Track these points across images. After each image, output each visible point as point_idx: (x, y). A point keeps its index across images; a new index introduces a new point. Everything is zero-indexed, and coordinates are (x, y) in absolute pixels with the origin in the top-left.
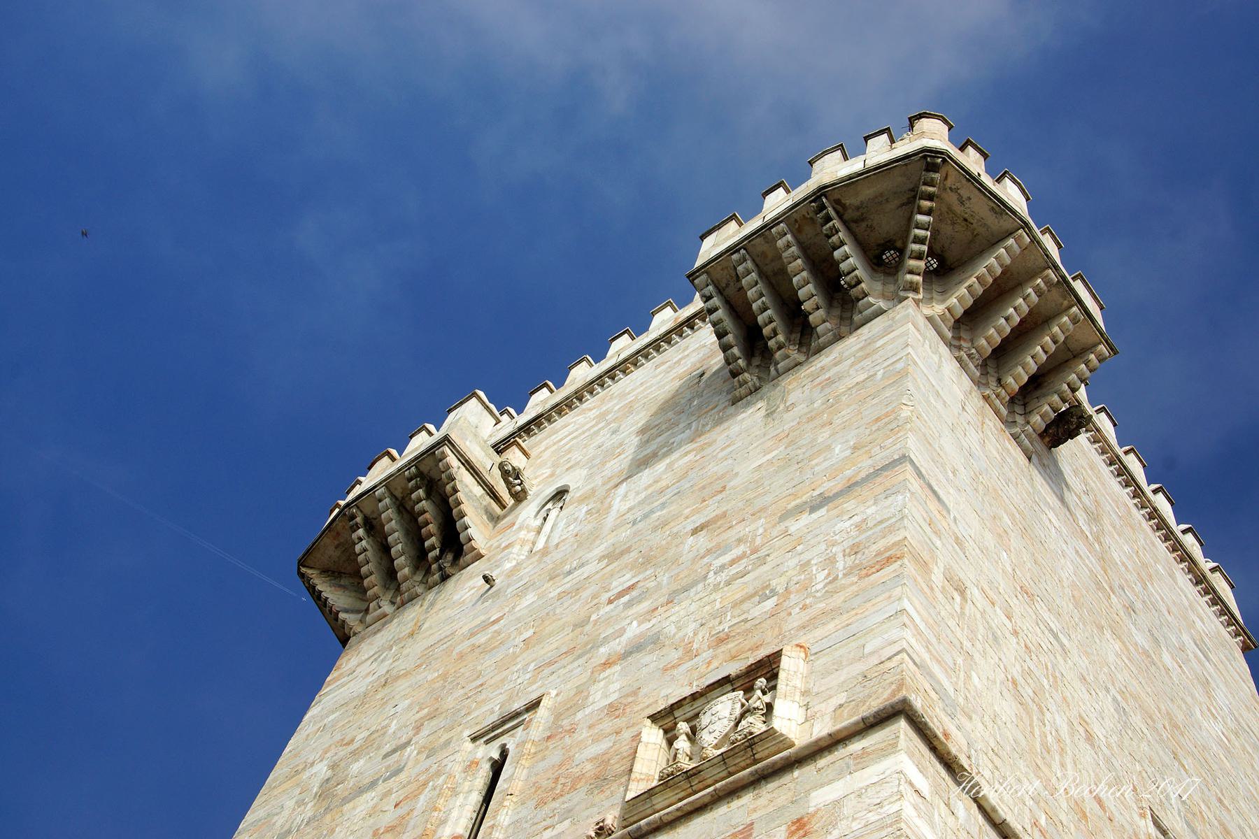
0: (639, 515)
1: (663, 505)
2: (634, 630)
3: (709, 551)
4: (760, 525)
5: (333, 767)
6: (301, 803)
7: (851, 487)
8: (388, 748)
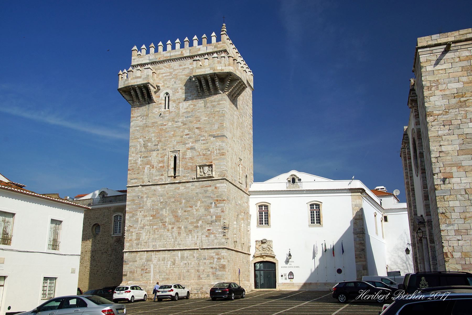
0: (186, 116)
2: (191, 144)
4: (206, 134)
5: (144, 141)
6: (141, 146)
7: (218, 136)
8: (154, 143)
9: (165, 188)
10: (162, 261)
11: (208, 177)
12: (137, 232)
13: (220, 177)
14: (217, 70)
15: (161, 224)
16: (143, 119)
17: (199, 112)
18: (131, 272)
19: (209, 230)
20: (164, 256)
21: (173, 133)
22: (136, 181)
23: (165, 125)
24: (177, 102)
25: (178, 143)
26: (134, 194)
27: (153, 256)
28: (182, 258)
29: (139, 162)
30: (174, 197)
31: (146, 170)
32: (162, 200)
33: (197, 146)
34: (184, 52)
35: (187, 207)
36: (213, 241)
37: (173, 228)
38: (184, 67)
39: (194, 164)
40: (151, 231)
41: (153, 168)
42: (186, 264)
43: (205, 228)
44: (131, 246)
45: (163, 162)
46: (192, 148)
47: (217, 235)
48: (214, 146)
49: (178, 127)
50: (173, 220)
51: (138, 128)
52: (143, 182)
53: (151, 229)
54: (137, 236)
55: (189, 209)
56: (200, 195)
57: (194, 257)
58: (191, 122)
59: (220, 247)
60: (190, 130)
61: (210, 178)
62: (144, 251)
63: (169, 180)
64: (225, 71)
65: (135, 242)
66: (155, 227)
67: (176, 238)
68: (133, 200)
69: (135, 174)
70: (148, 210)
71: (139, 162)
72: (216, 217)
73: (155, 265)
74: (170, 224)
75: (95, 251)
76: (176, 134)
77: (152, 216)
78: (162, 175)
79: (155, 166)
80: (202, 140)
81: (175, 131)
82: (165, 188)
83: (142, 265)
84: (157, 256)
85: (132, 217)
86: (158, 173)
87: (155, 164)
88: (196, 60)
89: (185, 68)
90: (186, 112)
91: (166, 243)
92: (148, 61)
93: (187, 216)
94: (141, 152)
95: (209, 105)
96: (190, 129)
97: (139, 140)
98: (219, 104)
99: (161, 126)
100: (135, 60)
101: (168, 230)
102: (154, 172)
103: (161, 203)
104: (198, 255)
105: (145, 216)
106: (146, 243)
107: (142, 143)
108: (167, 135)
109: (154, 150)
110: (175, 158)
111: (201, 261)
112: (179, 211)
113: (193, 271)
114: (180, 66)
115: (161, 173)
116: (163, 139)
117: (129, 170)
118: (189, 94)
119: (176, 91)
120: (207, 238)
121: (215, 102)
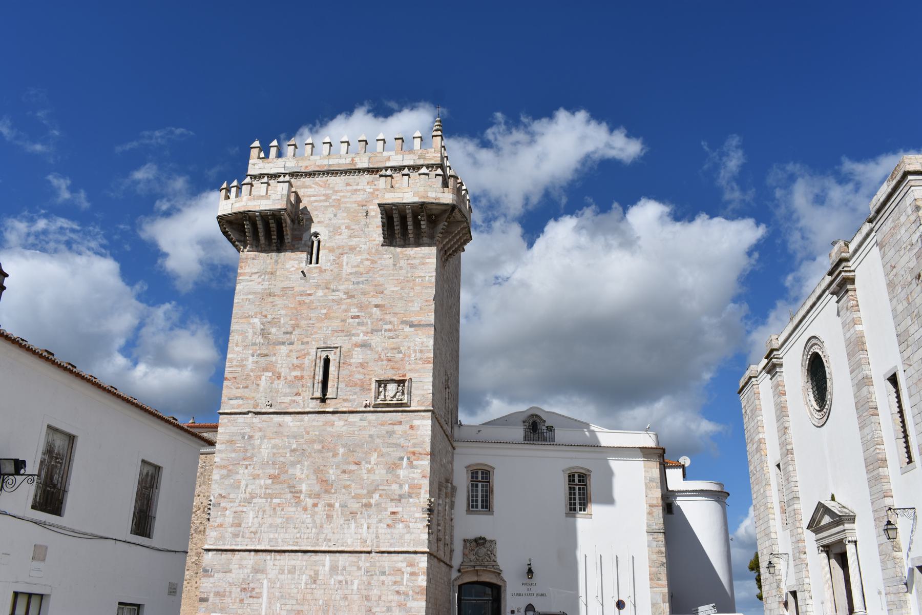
0: (355, 280)
1: (363, 283)
2: (362, 337)
3: (381, 320)
4: (395, 320)
6: (255, 333)
8: (283, 330)
9: (302, 421)
10: (289, 572)
11: (396, 405)
12: (234, 510)
13: (421, 405)
14: (427, 197)
15: (289, 496)
16: (263, 280)
17: (382, 276)
18: (217, 594)
19: (393, 513)
20: (293, 562)
21: (325, 311)
22: (240, 402)
23: (310, 295)
24: (338, 252)
25: (334, 331)
26: (234, 429)
27: (270, 563)
28: (334, 569)
29: (250, 363)
30: (321, 442)
31: (263, 382)
32: (294, 446)
33: (376, 340)
34: (357, 160)
35: (348, 463)
36: (402, 537)
37: (315, 505)
38: (355, 187)
39: (368, 377)
40: (267, 508)
41: (279, 378)
42: (340, 582)
43: (386, 509)
44: (222, 538)
45: (300, 367)
46: (364, 345)
47: (411, 525)
48: (412, 344)
49: (338, 302)
50: (317, 488)
51: (251, 297)
52: (256, 406)
53: (267, 504)
54: (234, 517)
55: (353, 467)
56: (378, 440)
57: (359, 568)
58: (364, 293)
59: (418, 550)
60: (361, 307)
61: (401, 407)
62: (250, 551)
63: (311, 405)
64: (442, 201)
65: (230, 530)
66: (276, 501)
67: (321, 527)
68: (231, 442)
69: (238, 388)
70: (264, 465)
71: (250, 363)
72: (410, 487)
73: (272, 582)
74: (310, 497)
76: (332, 315)
77: (270, 477)
78: (298, 394)
79: (283, 375)
80: (386, 330)
81: (330, 308)
82: (302, 421)
83: (244, 580)
84: (277, 563)
85: (228, 476)
86: (288, 390)
87: (284, 372)
88: (386, 176)
89: (356, 190)
90: (356, 273)
91: (298, 535)
92: (282, 171)
93: (348, 483)
94: (255, 344)
95: (402, 263)
96: (361, 307)
97: (252, 320)
98: (424, 264)
99: (301, 295)
100: (256, 165)
101: (305, 509)
102: (280, 386)
103: (293, 451)
104: (368, 565)
105: (256, 477)
106: (255, 533)
107: (259, 326)
108: (312, 315)
109: (284, 343)
110: (327, 361)
111: (375, 577)
112: (331, 472)
113: (356, 597)
114: (348, 184)
115: (295, 390)
116: (303, 323)
117: (226, 379)
118: (363, 240)
119: (336, 231)
120: (389, 530)
121: (415, 258)
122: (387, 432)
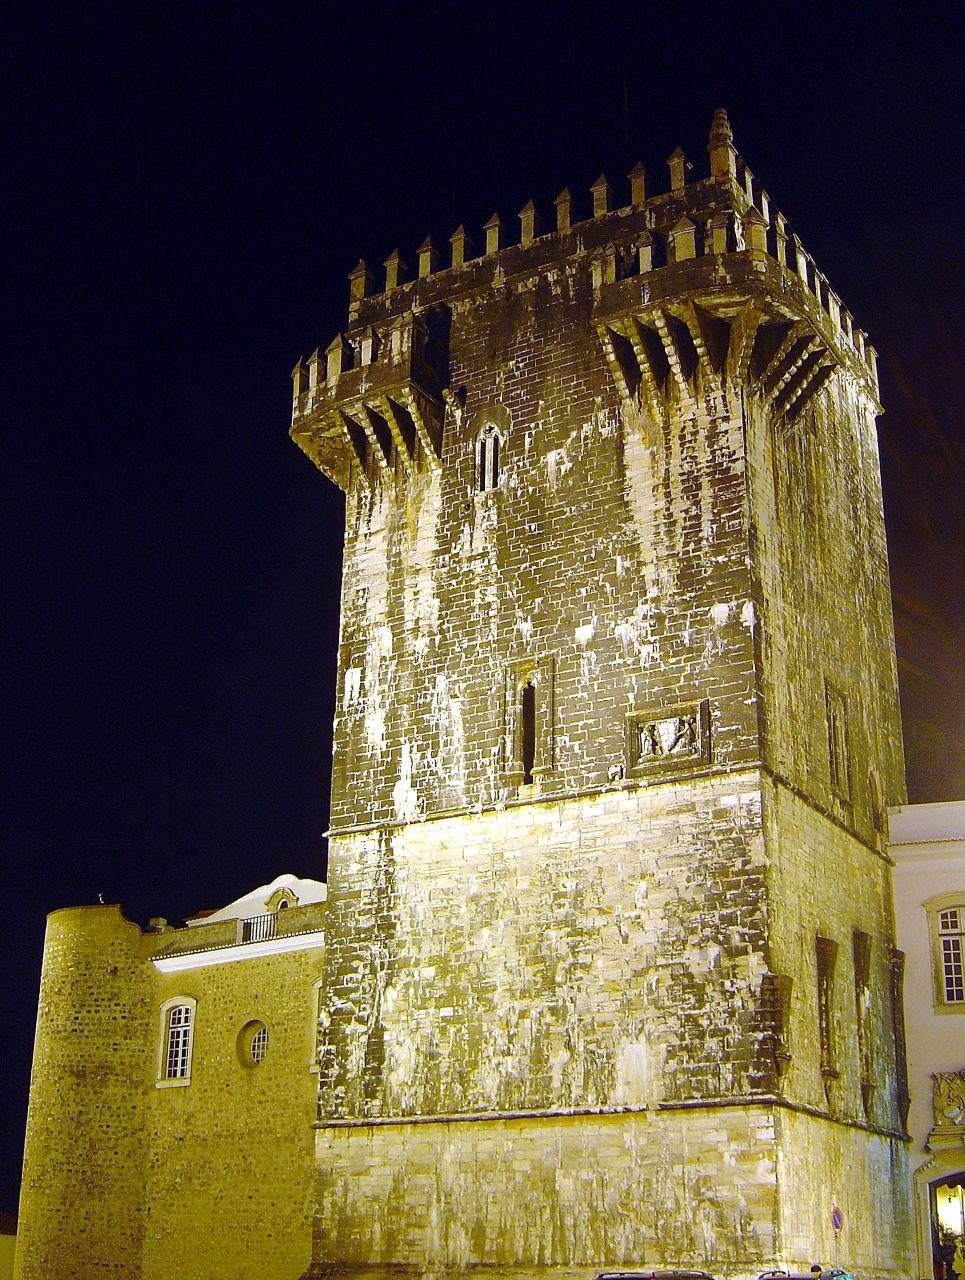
57: (625, 1151)
75: (250, 1133)
104: (643, 1141)
110: (529, 694)
122: (666, 831)
